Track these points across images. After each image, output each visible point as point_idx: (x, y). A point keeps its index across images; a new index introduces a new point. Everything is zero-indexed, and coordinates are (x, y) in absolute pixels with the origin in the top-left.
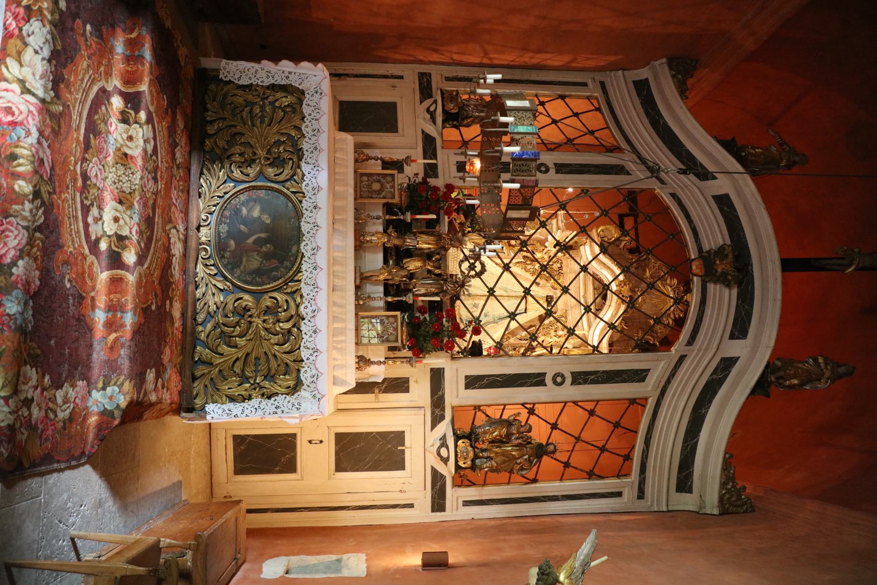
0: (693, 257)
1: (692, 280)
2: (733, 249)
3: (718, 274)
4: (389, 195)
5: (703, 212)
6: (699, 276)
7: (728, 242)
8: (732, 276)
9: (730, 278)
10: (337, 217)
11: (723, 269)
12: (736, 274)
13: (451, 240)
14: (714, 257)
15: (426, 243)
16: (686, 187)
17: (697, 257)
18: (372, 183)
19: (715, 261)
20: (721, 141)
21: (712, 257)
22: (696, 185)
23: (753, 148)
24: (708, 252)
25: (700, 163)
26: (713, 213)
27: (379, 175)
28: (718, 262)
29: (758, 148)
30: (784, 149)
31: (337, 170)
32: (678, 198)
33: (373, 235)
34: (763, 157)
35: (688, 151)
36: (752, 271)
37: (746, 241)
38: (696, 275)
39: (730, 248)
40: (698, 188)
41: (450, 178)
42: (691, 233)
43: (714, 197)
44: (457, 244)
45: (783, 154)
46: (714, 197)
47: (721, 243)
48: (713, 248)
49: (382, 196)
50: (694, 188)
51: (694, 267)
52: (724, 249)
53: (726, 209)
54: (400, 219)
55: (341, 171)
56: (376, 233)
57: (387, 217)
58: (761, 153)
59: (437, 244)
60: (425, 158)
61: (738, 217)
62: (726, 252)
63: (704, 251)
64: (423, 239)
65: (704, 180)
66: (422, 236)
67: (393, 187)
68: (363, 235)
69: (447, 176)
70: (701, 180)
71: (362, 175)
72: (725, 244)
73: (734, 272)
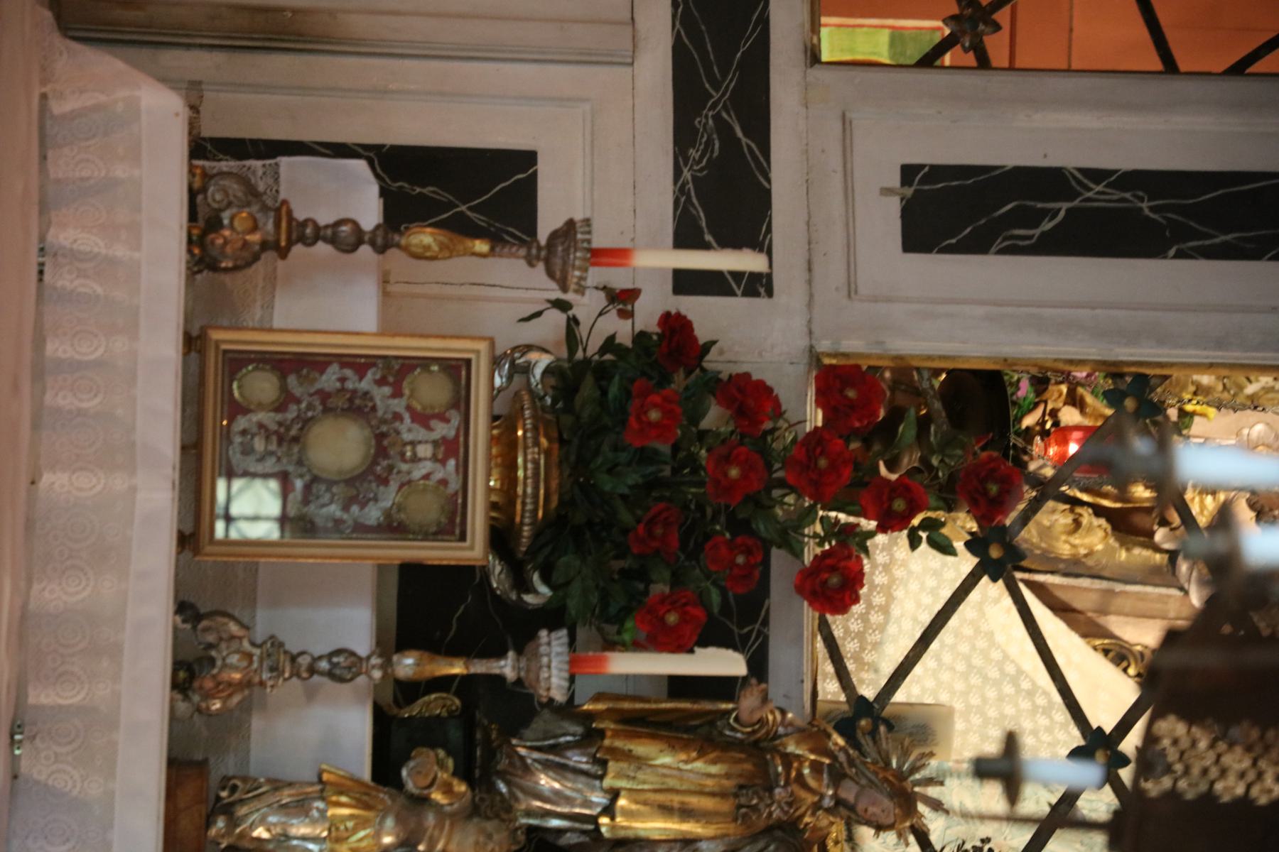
4: (427, 510)
10: (40, 696)
13: (837, 777)
15: (666, 810)
18: (306, 423)
27: (359, 365)
31: (55, 348)
33: (300, 807)
41: (851, 290)
44: (883, 806)
49: (373, 514)
54: (500, 679)
55: (89, 351)
56: (325, 788)
57: (407, 664)
59: (741, 814)
60: (686, 238)
64: (647, 781)
66: (641, 748)
67: (454, 448)
68: (228, 810)
69: (832, 271)
71: (236, 362)
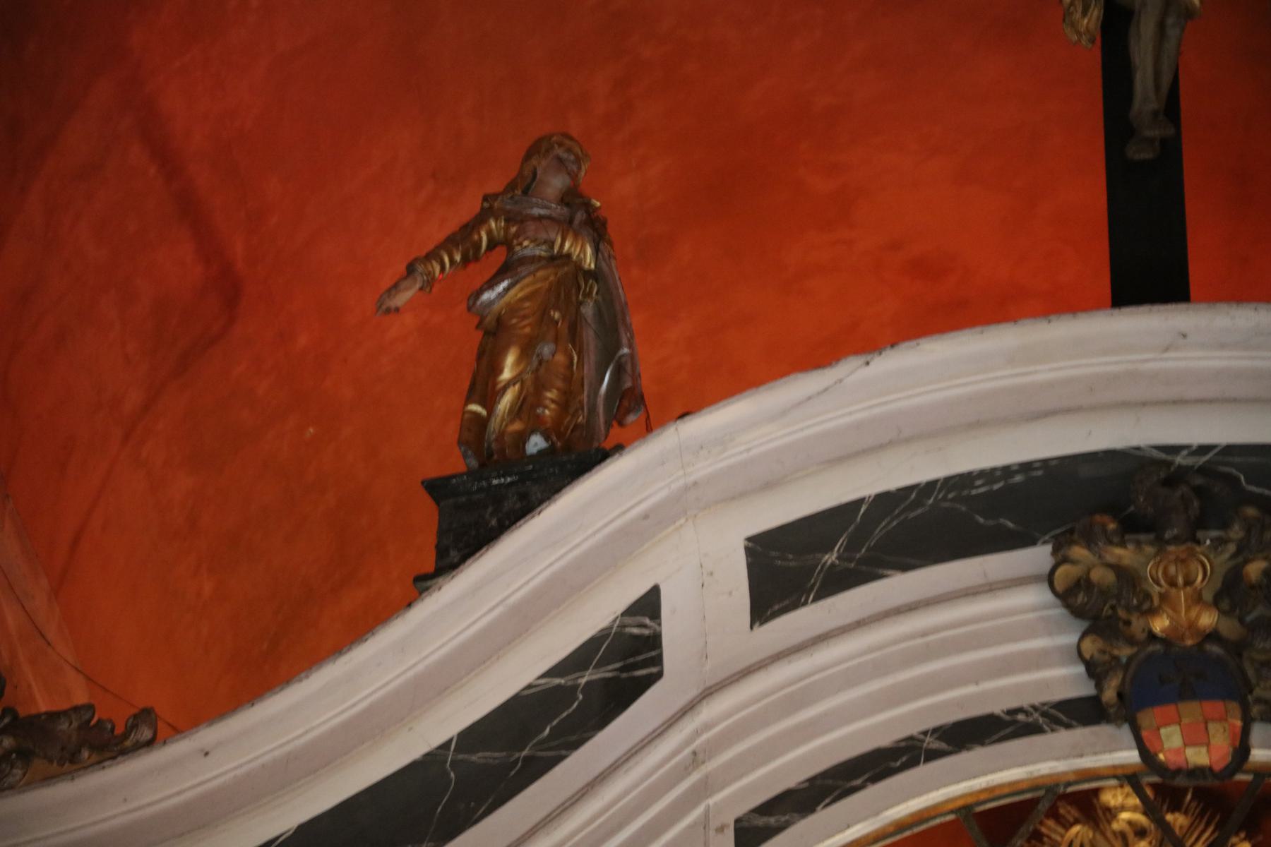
0: (1130, 756)
1: (1263, 772)
2: (1089, 540)
3: (1230, 628)
5: (852, 678)
6: (1246, 732)
7: (1038, 556)
8: (1244, 552)
9: (1254, 569)
11: (1198, 599)
12: (1236, 532)
14: (1131, 641)
16: (696, 760)
17: (1125, 732)
19: (1152, 637)
20: (441, 552)
21: (1124, 652)
22: (689, 708)
23: (485, 390)
24: (1094, 670)
25: (549, 673)
26: (859, 624)
28: (1160, 624)
29: (497, 369)
30: (492, 244)
32: (767, 808)
34: (547, 350)
35: (473, 737)
36: (1203, 449)
37: (1026, 467)
38: (1242, 751)
39: (1078, 552)
40: (708, 693)
42: (976, 755)
43: (762, 609)
45: (527, 248)
46: (762, 609)
47: (1037, 596)
48: (1071, 639)
50: (708, 712)
51: (1198, 757)
52: (1082, 584)
53: (831, 558)
58: (525, 354)
61: (886, 501)
62: (1100, 575)
63: (1085, 689)
65: (658, 660)
70: (659, 675)
72: (1050, 579)
73: (1219, 543)
